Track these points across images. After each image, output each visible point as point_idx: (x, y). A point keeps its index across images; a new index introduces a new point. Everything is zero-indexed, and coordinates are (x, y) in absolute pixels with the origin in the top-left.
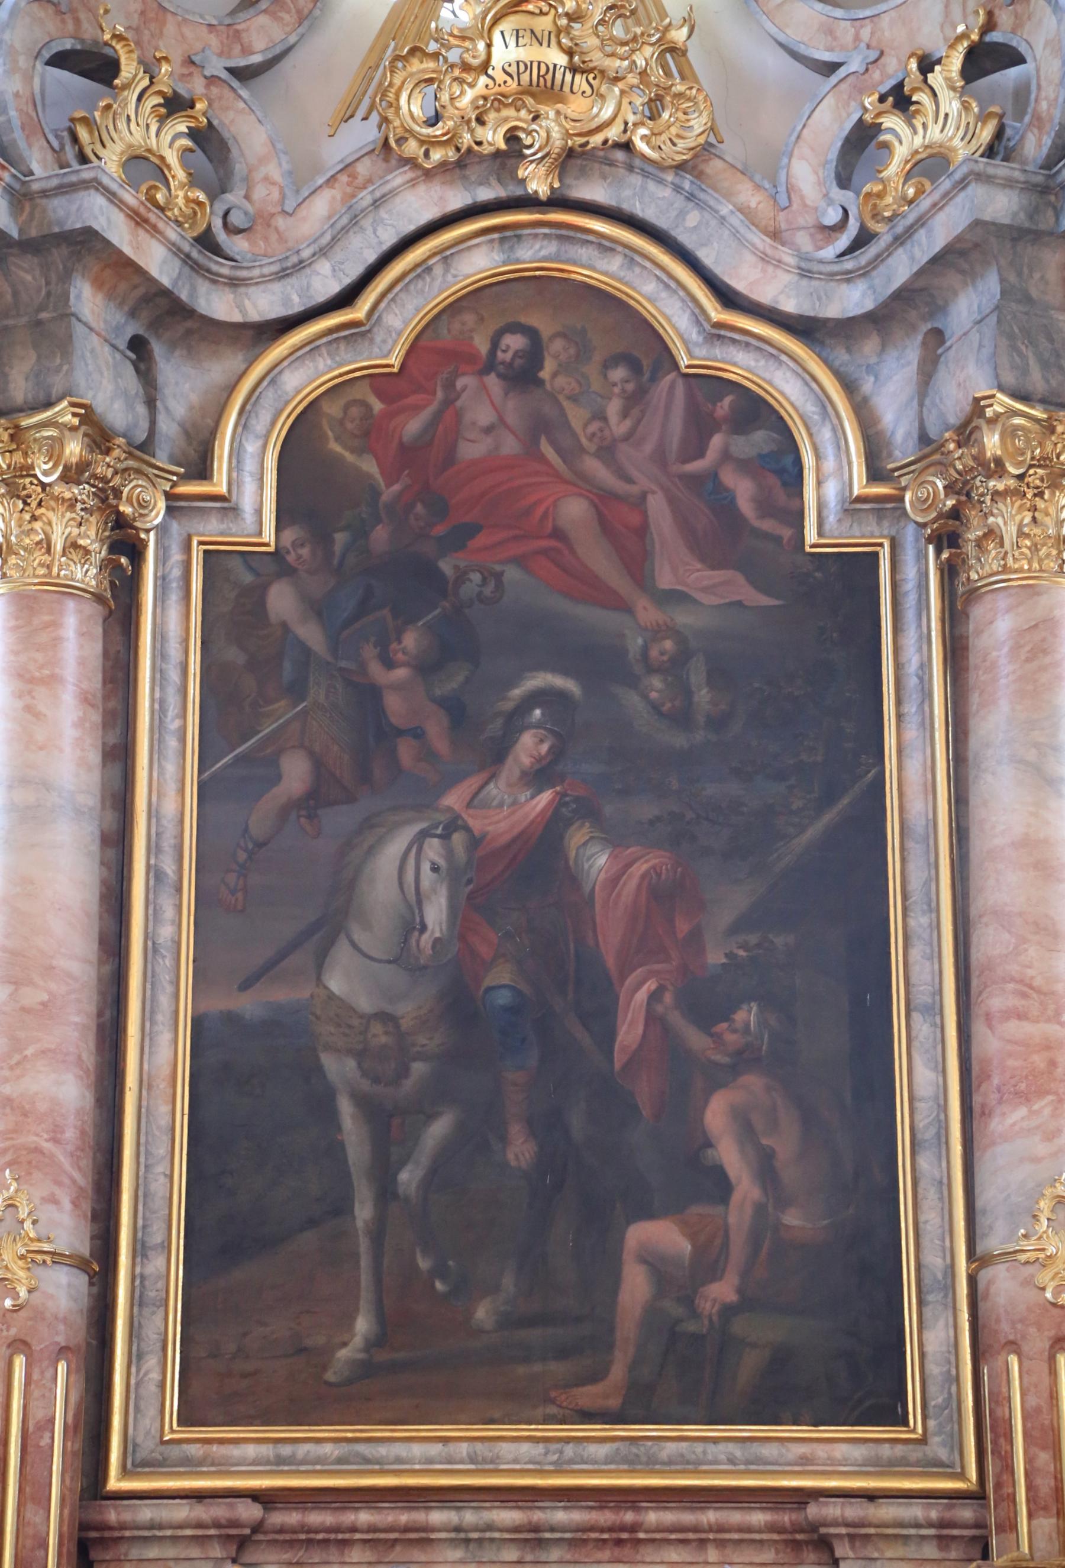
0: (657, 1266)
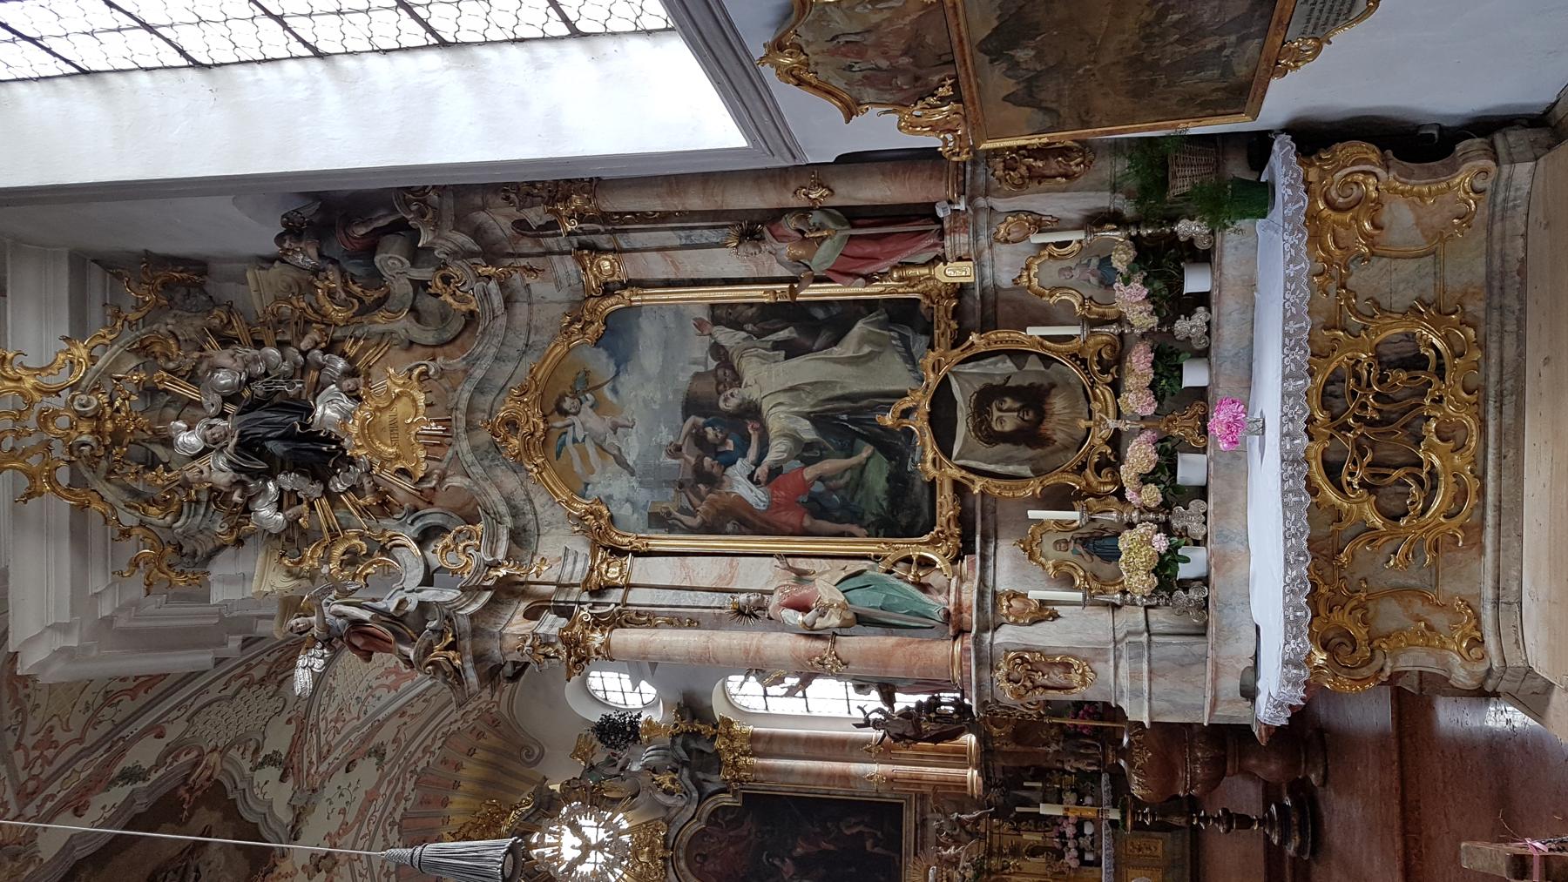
0: (875, 845)
